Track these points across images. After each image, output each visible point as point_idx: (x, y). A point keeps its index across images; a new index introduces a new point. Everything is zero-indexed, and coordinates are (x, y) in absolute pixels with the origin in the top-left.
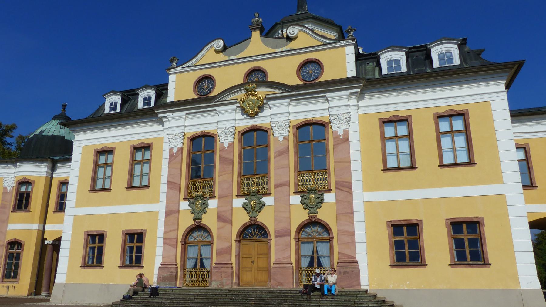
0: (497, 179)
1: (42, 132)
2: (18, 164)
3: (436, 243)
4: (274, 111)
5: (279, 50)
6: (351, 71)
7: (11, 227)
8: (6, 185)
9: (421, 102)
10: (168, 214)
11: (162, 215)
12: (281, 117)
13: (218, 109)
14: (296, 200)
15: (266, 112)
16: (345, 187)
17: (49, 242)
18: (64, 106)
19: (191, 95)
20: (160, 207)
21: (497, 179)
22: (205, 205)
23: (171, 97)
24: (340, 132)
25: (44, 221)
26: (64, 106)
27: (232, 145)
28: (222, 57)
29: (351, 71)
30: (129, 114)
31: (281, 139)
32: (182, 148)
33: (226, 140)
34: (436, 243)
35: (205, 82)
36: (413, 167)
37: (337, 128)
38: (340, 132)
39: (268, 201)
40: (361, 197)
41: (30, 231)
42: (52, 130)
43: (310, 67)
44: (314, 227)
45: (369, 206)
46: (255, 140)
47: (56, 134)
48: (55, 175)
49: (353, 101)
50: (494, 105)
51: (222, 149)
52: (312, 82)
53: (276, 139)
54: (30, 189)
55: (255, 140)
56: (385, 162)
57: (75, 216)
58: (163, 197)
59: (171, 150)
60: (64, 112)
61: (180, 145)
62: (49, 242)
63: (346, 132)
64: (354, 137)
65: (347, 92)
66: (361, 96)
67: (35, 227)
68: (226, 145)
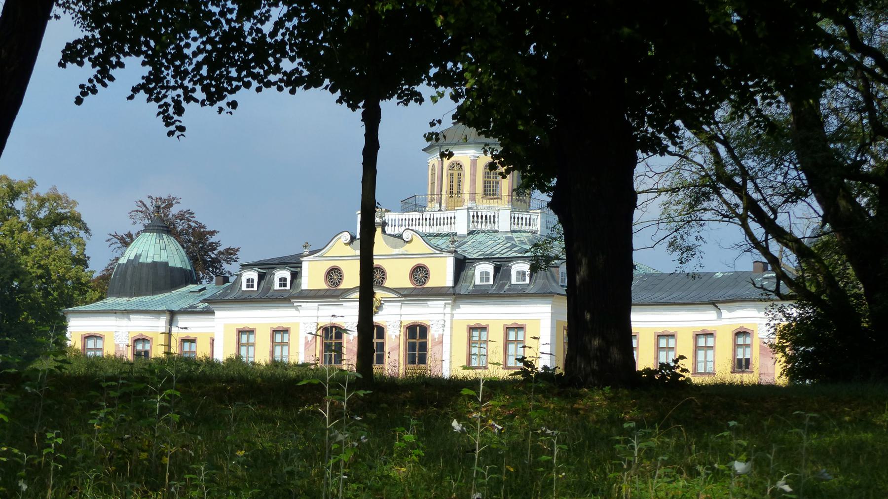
1: (137, 257)
2: (131, 316)
5: (396, 251)
8: (117, 341)
19: (322, 285)
24: (436, 336)
31: (393, 337)
38: (436, 336)
42: (151, 254)
43: (419, 272)
47: (157, 260)
48: (174, 330)
49: (448, 309)
54: (147, 347)
56: (469, 362)
65: (443, 303)
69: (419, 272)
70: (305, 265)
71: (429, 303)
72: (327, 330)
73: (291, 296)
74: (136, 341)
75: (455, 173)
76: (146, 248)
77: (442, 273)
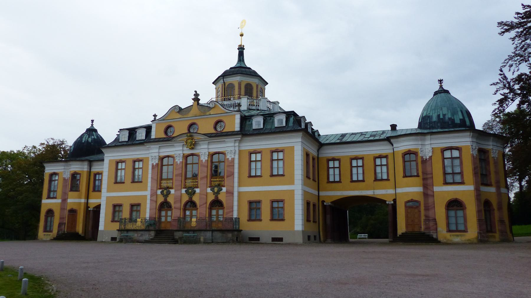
0: (292, 182)
4: (202, 147)
6: (237, 128)
7: (69, 201)
8: (65, 176)
10: (151, 196)
11: (149, 197)
12: (204, 150)
13: (175, 144)
14: (209, 190)
15: (198, 147)
17: (91, 209)
18: (92, 121)
20: (148, 193)
21: (292, 182)
22: (169, 193)
23: (153, 136)
24: (230, 159)
25: (88, 198)
26: (92, 121)
28: (179, 116)
32: (158, 164)
33: (179, 160)
37: (229, 157)
38: (230, 159)
39: (198, 190)
41: (80, 203)
44: (217, 204)
50: (296, 148)
57: (107, 197)
58: (149, 189)
59: (153, 164)
61: (157, 162)
62: (91, 209)
63: (233, 159)
64: (236, 162)
66: (240, 141)
67: (83, 201)
71: (226, 140)
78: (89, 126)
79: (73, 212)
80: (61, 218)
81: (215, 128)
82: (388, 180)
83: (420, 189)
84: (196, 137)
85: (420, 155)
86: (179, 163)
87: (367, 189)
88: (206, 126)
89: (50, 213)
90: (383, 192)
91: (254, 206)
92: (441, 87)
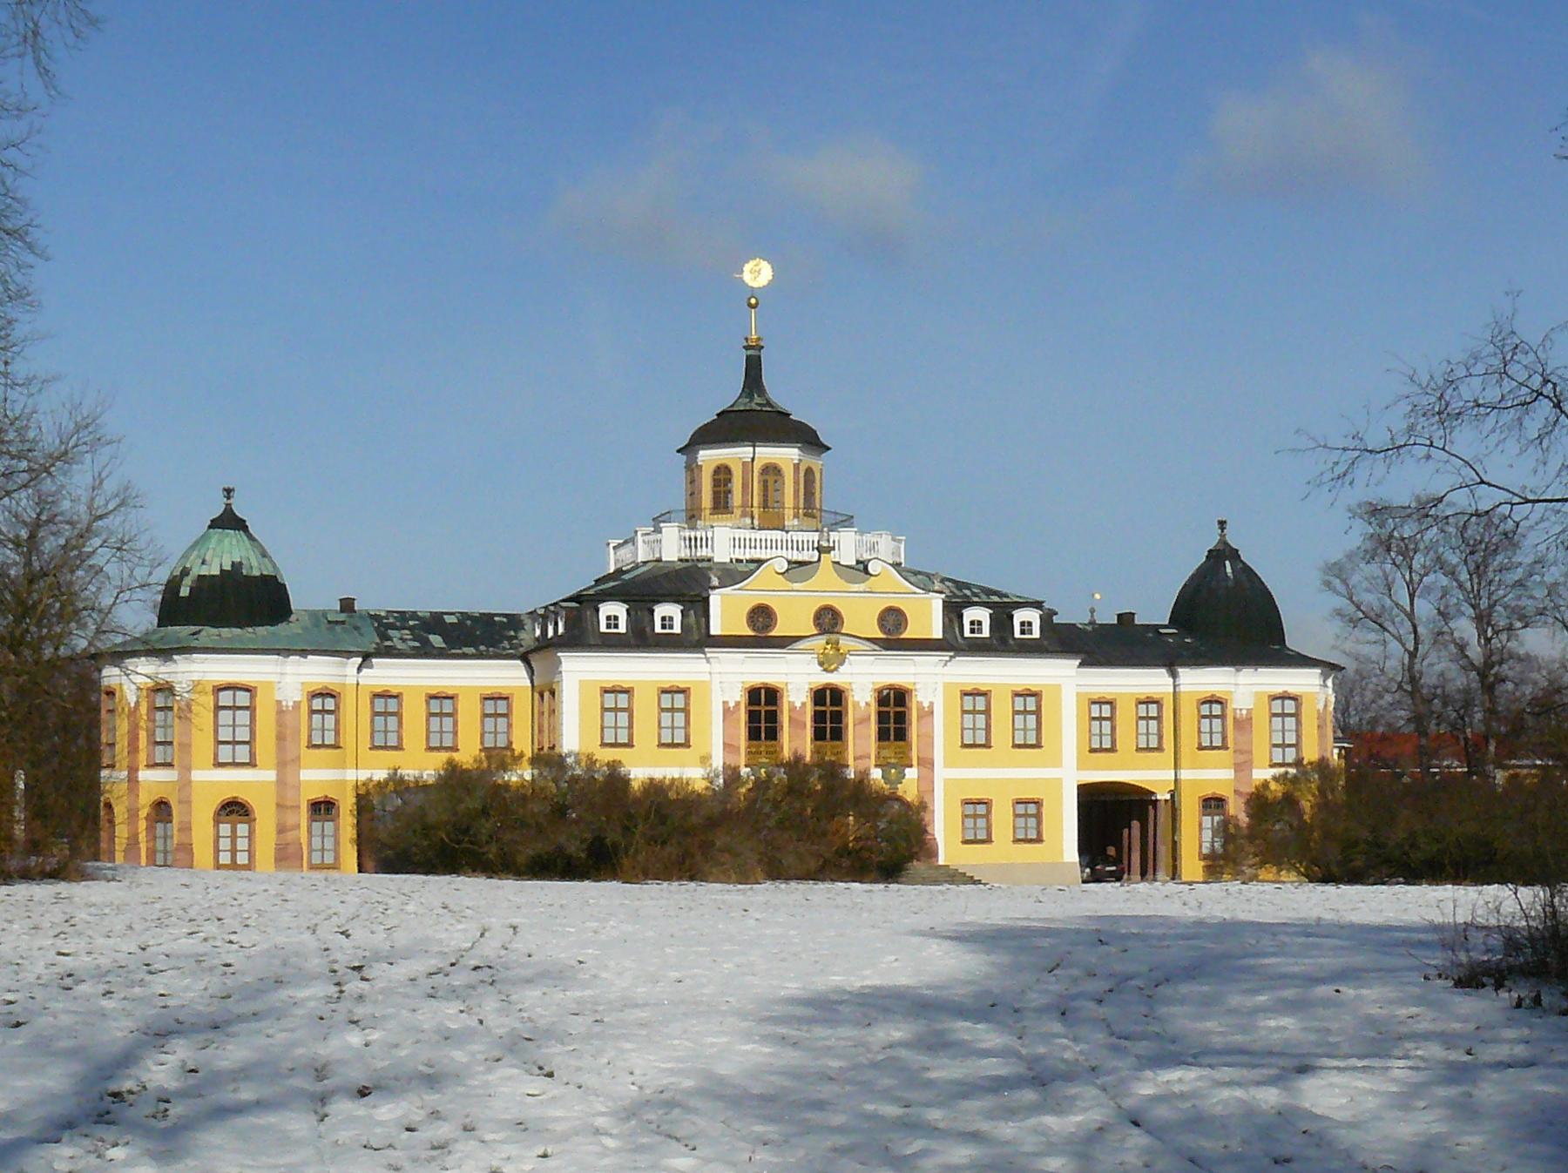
0: (1057, 763)
3: (1003, 820)
6: (937, 634)
7: (306, 775)
9: (1003, 674)
12: (863, 678)
16: (927, 763)
18: (228, 492)
21: (1057, 763)
23: (715, 630)
24: (926, 705)
26: (228, 492)
27: (804, 704)
29: (937, 634)
30: (641, 639)
31: (863, 704)
34: (1003, 820)
35: (761, 615)
36: (987, 746)
37: (921, 697)
38: (926, 705)
40: (941, 773)
42: (255, 564)
43: (892, 618)
45: (947, 781)
46: (829, 703)
49: (939, 669)
51: (792, 709)
52: (893, 635)
53: (856, 704)
55: (829, 703)
60: (228, 510)
63: (932, 704)
68: (798, 705)
69: (892, 618)
70: (715, 599)
72: (754, 694)
73: (697, 639)
74: (315, 695)
75: (771, 479)
76: (244, 554)
77: (928, 617)
78: (218, 511)
79: (323, 808)
80: (281, 830)
81: (882, 626)
82: (1159, 749)
83: (1227, 774)
84: (845, 643)
85: (1232, 706)
86: (798, 705)
87: (1123, 767)
88: (861, 617)
89: (234, 809)
90: (1152, 776)
91: (977, 809)
92: (1223, 536)
